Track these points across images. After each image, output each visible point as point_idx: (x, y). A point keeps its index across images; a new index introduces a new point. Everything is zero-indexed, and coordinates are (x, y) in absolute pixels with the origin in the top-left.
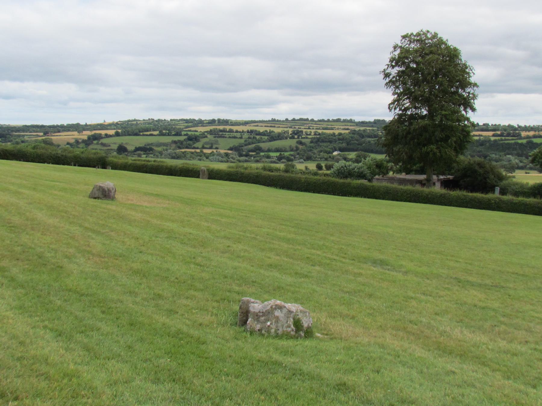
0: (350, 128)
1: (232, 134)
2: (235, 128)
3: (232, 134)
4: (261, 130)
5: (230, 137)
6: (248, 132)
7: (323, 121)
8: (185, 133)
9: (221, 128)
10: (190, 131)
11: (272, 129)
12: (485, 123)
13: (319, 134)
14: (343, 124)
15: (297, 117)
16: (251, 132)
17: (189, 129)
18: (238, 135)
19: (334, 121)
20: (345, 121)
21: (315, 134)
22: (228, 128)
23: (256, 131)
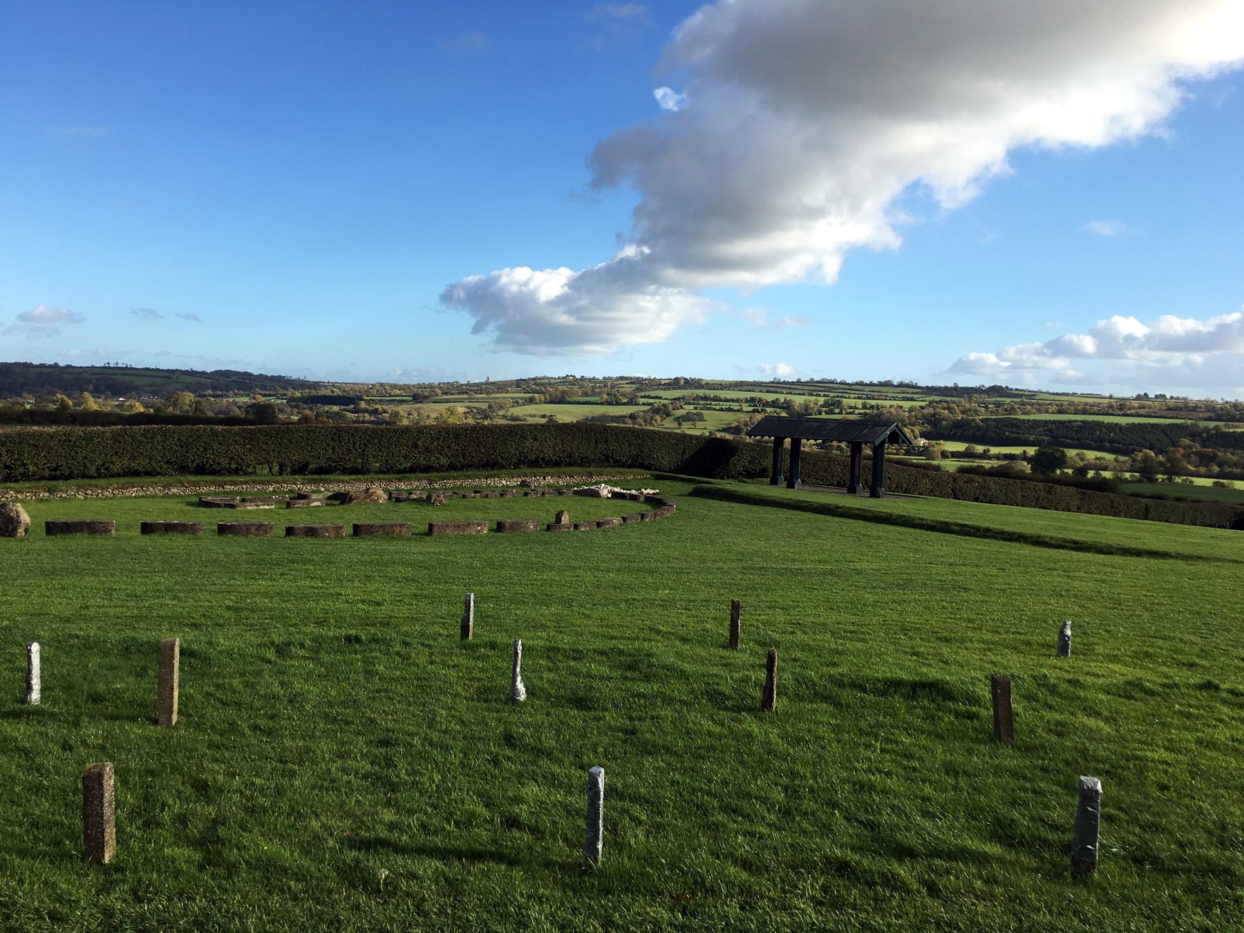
0: (915, 396)
1: (726, 405)
2: (724, 394)
3: (726, 405)
4: (770, 397)
5: (721, 410)
6: (747, 401)
7: (861, 384)
8: (645, 400)
9: (701, 392)
10: (649, 397)
11: (789, 397)
12: (1158, 393)
13: (872, 407)
14: (899, 390)
15: (817, 378)
16: (753, 399)
17: (647, 393)
18: (735, 406)
19: (881, 384)
20: (901, 385)
21: (864, 407)
22: (712, 393)
23: (760, 400)
